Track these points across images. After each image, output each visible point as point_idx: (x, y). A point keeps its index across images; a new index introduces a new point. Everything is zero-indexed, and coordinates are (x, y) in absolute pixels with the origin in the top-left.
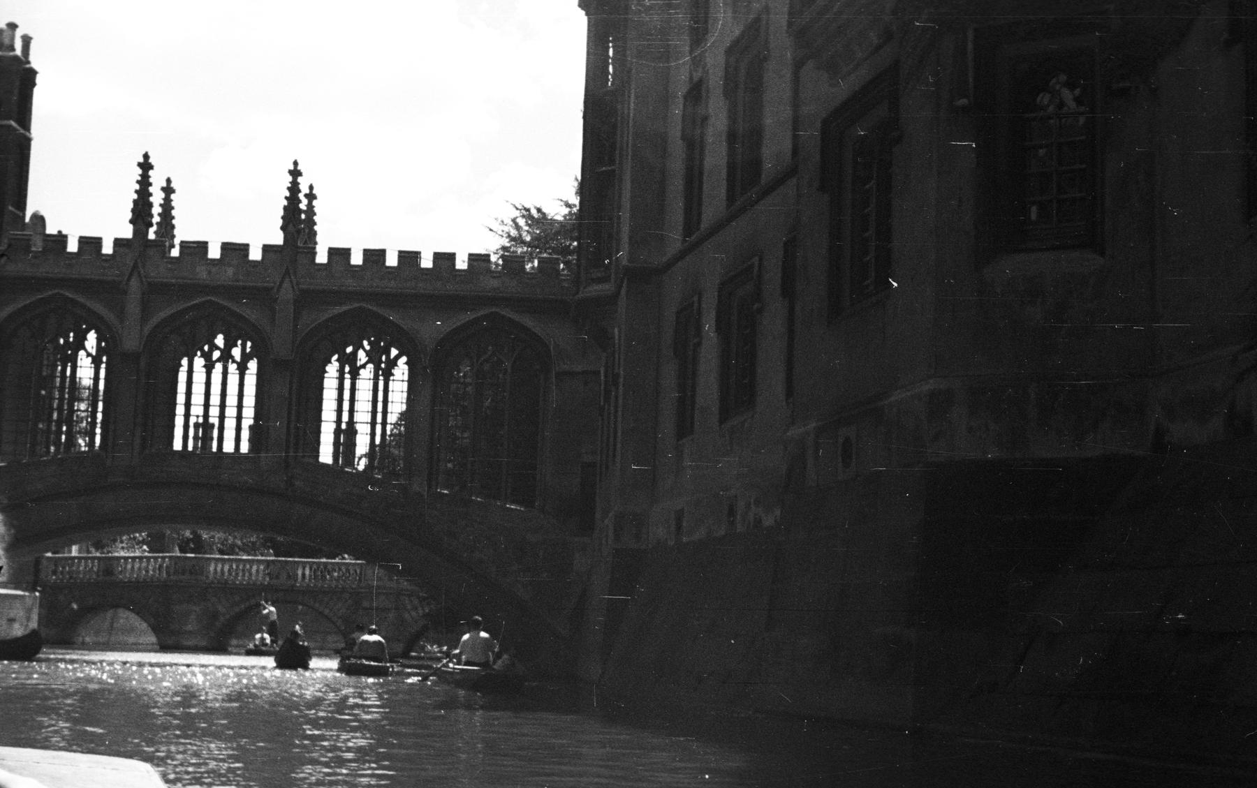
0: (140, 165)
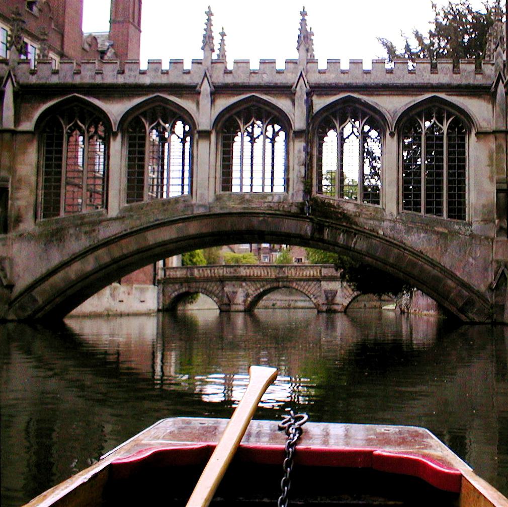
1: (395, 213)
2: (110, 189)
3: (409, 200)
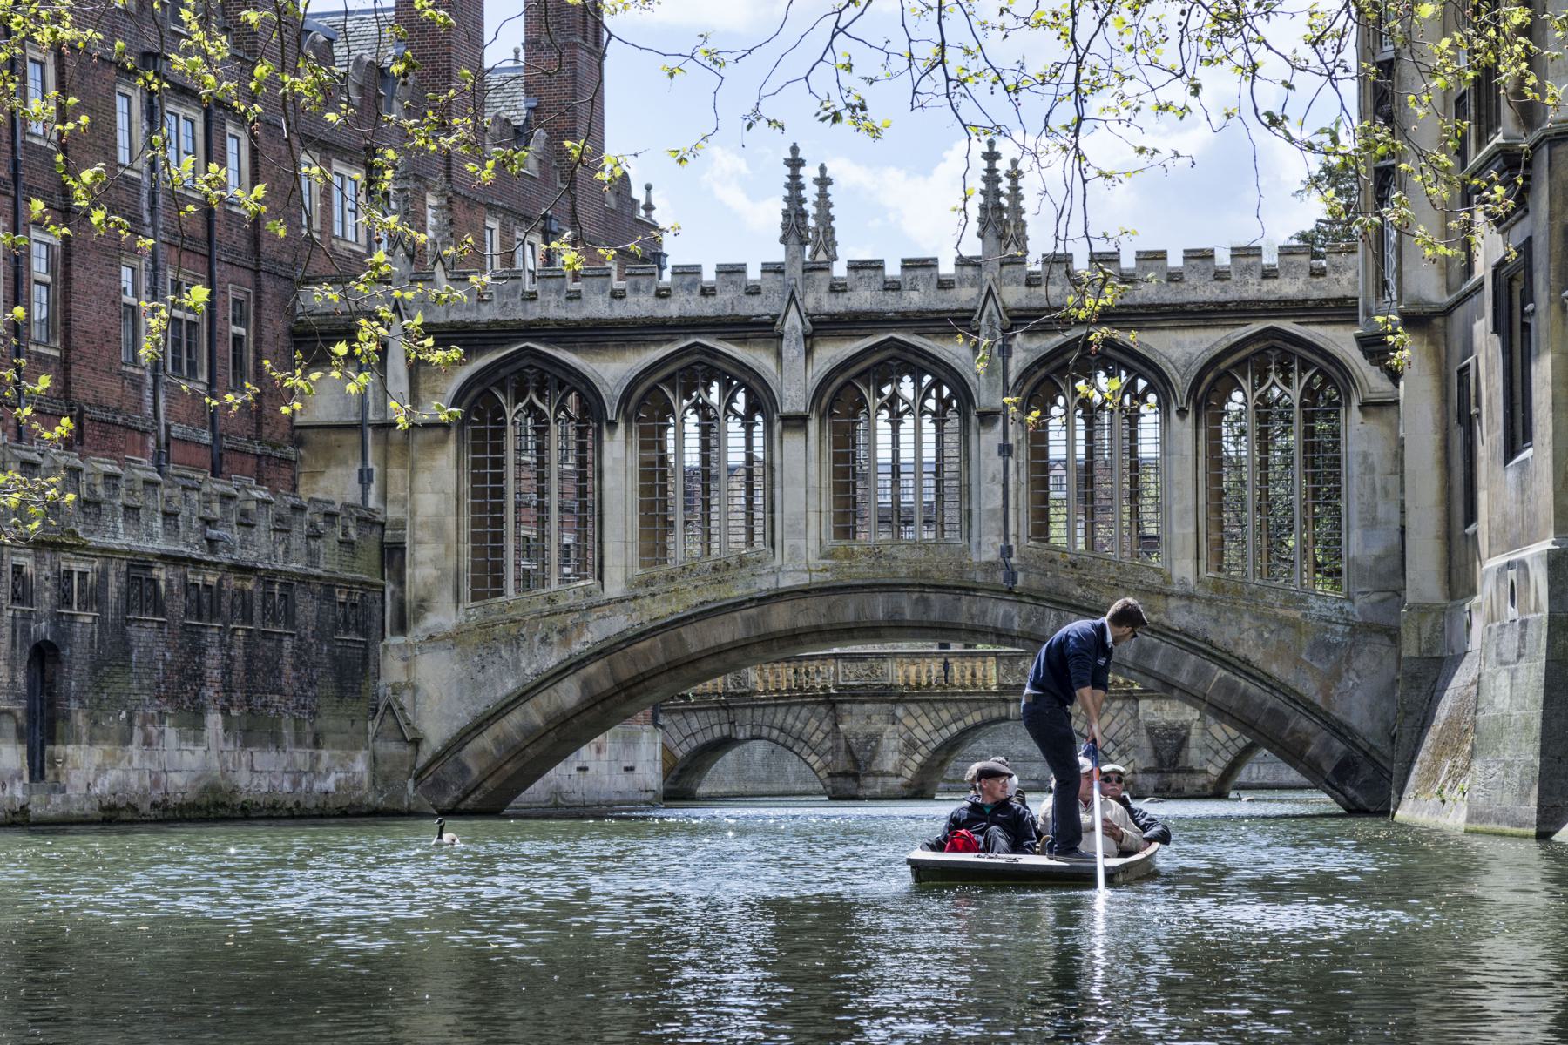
0: (787, 162)
1: (1191, 579)
2: (606, 539)
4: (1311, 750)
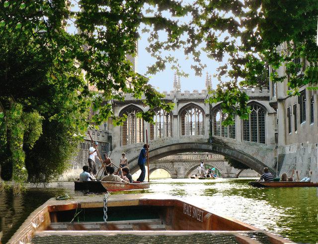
3: (246, 137)
4: (260, 170)
